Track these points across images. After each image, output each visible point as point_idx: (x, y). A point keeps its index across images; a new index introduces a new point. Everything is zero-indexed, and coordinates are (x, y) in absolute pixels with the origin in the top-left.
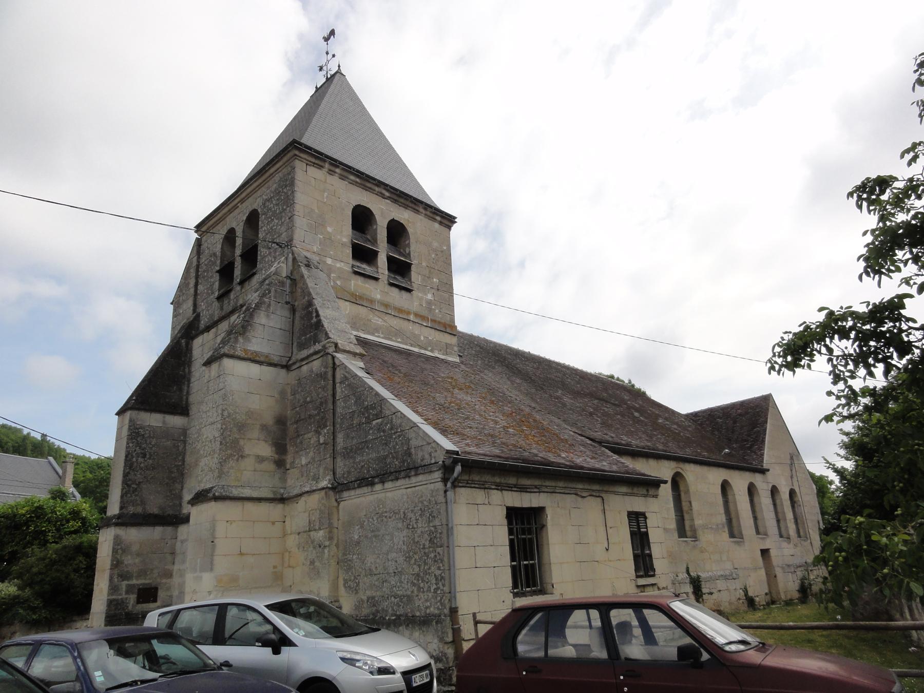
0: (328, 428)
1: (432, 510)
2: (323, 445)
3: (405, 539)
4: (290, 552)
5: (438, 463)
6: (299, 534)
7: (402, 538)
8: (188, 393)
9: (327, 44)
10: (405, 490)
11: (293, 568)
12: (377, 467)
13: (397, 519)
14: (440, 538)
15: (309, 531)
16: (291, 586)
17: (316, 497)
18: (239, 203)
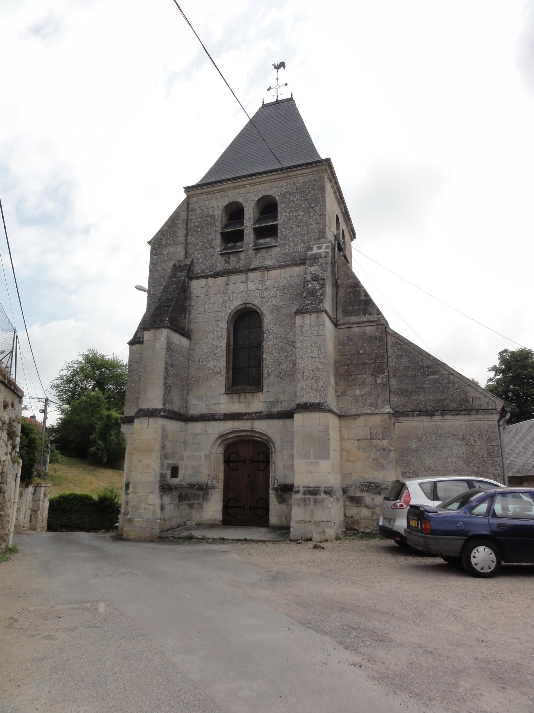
0: (385, 374)
1: (490, 436)
2: (381, 385)
3: (464, 451)
4: (347, 451)
5: (497, 409)
6: (358, 440)
7: (461, 450)
8: (189, 322)
9: (277, 72)
10: (464, 422)
11: (353, 462)
12: (435, 405)
13: (456, 439)
14: (497, 453)
15: (371, 439)
16: (351, 474)
17: (379, 418)
18: (249, 184)
